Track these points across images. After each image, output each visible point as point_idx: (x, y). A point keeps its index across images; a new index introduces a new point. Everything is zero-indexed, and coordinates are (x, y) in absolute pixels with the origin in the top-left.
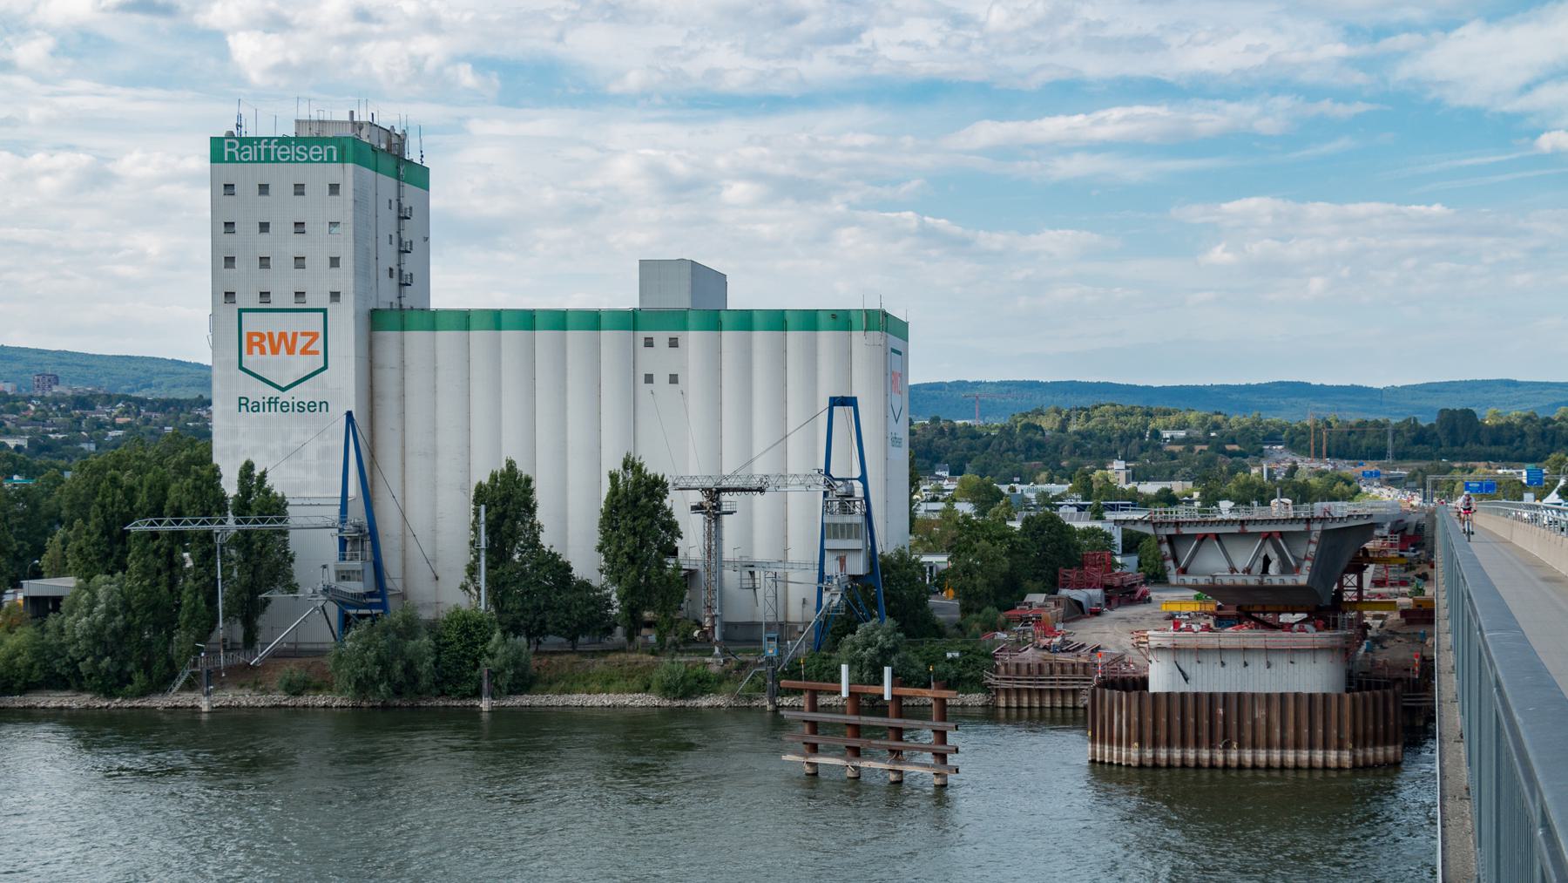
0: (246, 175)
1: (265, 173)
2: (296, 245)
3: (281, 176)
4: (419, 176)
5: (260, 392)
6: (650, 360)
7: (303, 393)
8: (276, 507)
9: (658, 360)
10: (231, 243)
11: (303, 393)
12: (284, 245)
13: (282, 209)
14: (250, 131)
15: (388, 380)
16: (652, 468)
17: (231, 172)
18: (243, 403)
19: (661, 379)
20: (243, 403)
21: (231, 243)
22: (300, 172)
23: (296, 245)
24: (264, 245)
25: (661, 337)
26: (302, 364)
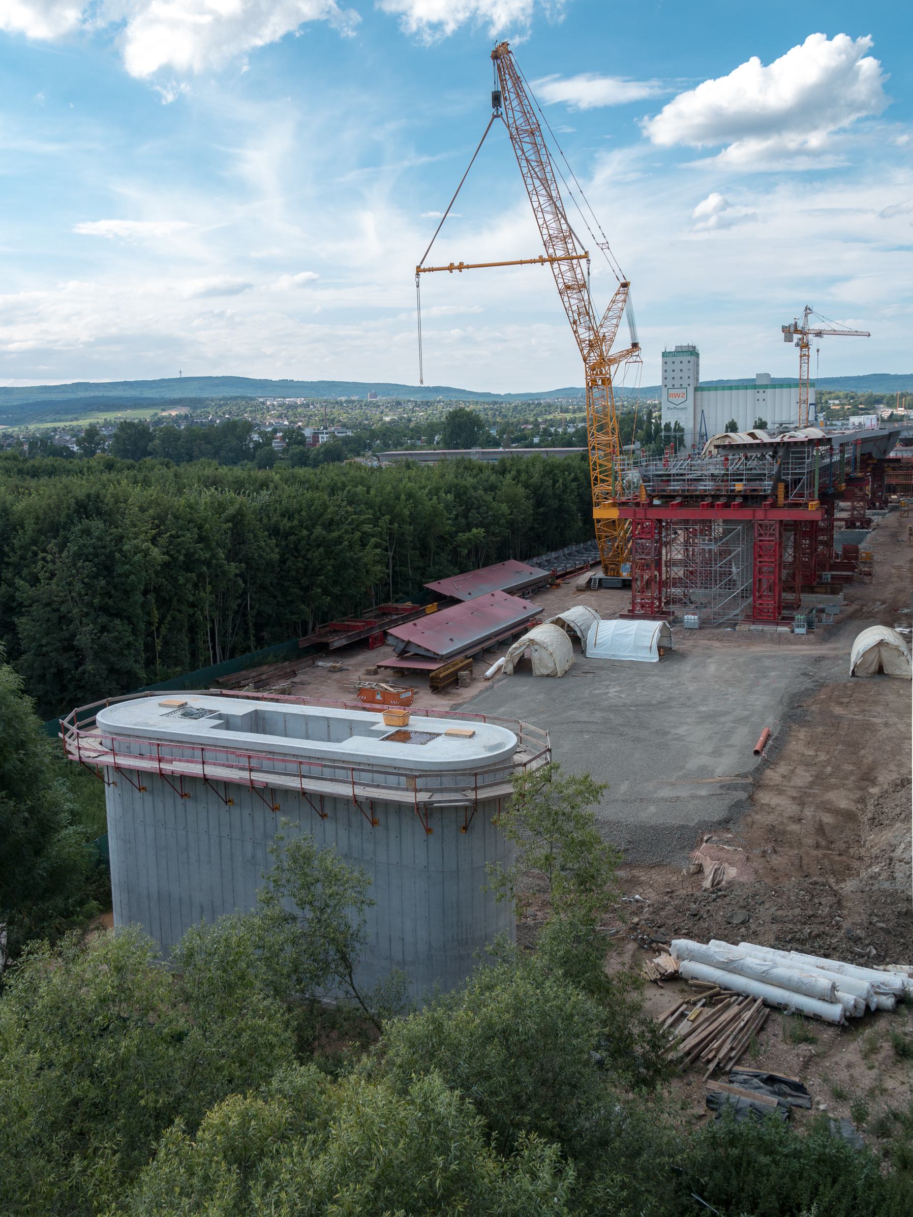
1: (674, 359)
2: (681, 374)
3: (677, 359)
4: (697, 355)
5: (672, 406)
6: (758, 396)
7: (681, 406)
8: (682, 430)
9: (761, 396)
11: (681, 406)
12: (677, 374)
13: (677, 367)
14: (668, 350)
16: (764, 420)
17: (666, 359)
18: (668, 408)
19: (761, 400)
20: (668, 408)
23: (681, 374)
24: (673, 374)
25: (761, 391)
26: (682, 400)
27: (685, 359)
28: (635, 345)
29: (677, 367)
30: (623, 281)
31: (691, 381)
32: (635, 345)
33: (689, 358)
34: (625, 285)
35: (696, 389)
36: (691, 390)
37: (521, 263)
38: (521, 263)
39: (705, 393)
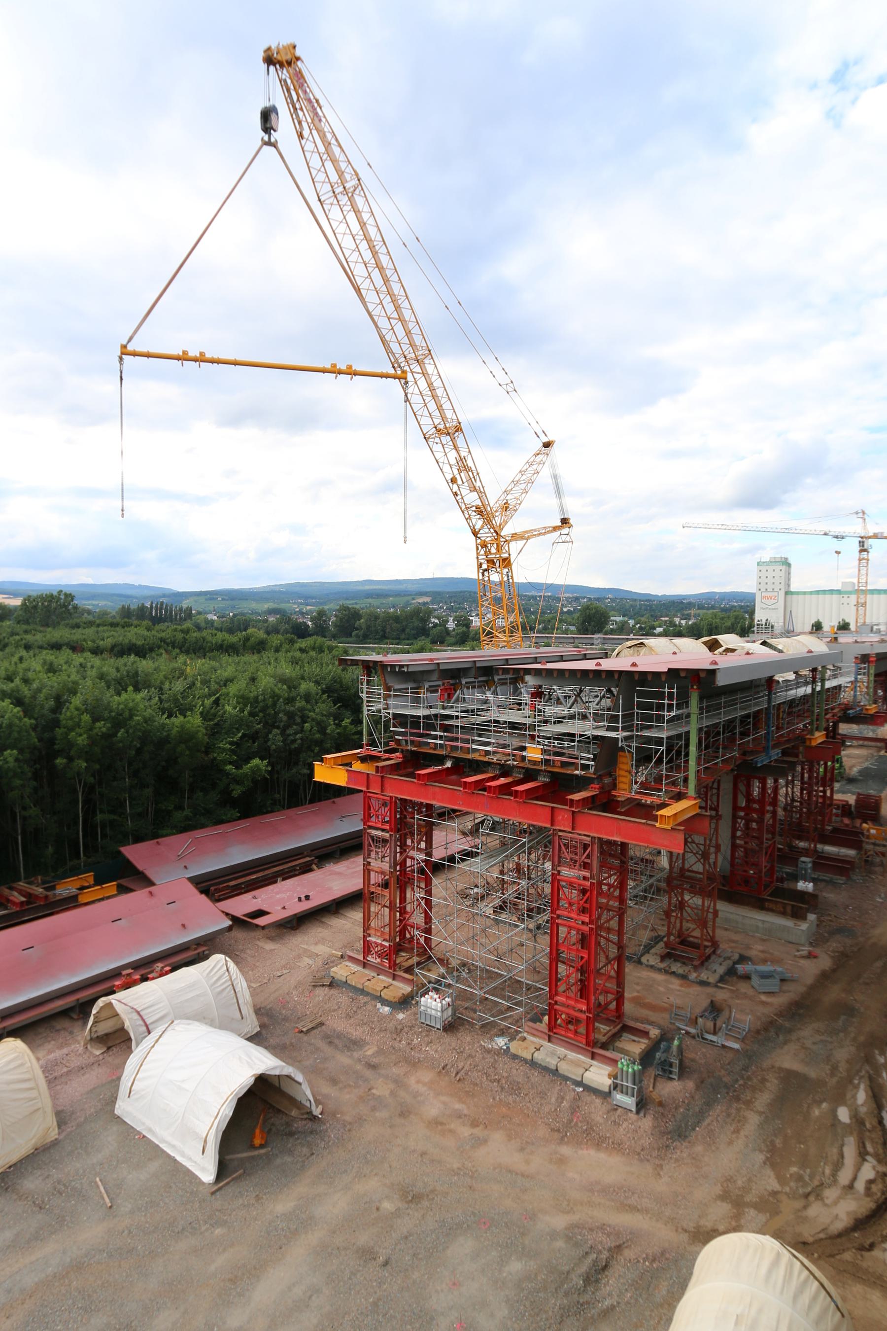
0: (763, 568)
1: (767, 568)
2: (773, 580)
3: (770, 568)
6: (843, 600)
7: (773, 606)
9: (845, 600)
10: (760, 580)
11: (773, 606)
15: (788, 604)
16: (847, 621)
21: (760, 580)
22: (774, 568)
23: (773, 580)
25: (846, 596)
26: (773, 601)
27: (778, 568)
28: (565, 521)
29: (770, 574)
30: (545, 440)
31: (782, 586)
32: (565, 521)
33: (781, 567)
34: (547, 445)
35: (787, 593)
36: (782, 594)
37: (235, 363)
38: (235, 363)
39: (794, 596)
